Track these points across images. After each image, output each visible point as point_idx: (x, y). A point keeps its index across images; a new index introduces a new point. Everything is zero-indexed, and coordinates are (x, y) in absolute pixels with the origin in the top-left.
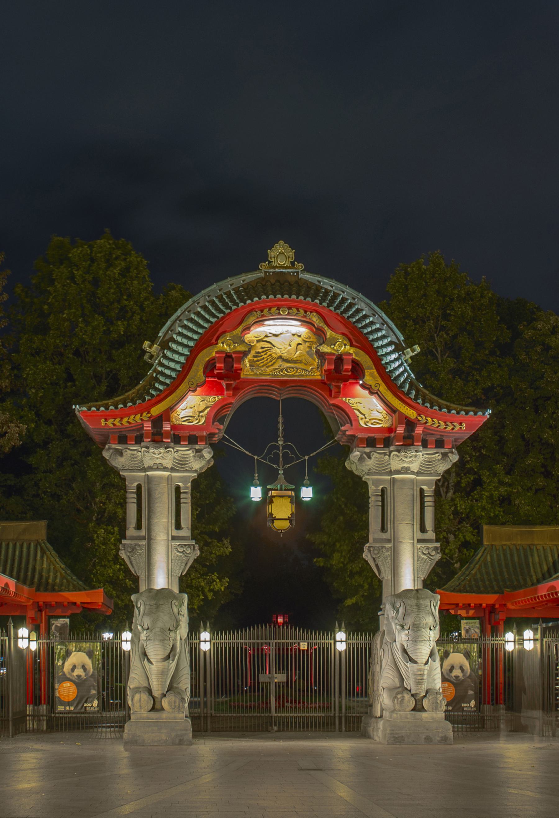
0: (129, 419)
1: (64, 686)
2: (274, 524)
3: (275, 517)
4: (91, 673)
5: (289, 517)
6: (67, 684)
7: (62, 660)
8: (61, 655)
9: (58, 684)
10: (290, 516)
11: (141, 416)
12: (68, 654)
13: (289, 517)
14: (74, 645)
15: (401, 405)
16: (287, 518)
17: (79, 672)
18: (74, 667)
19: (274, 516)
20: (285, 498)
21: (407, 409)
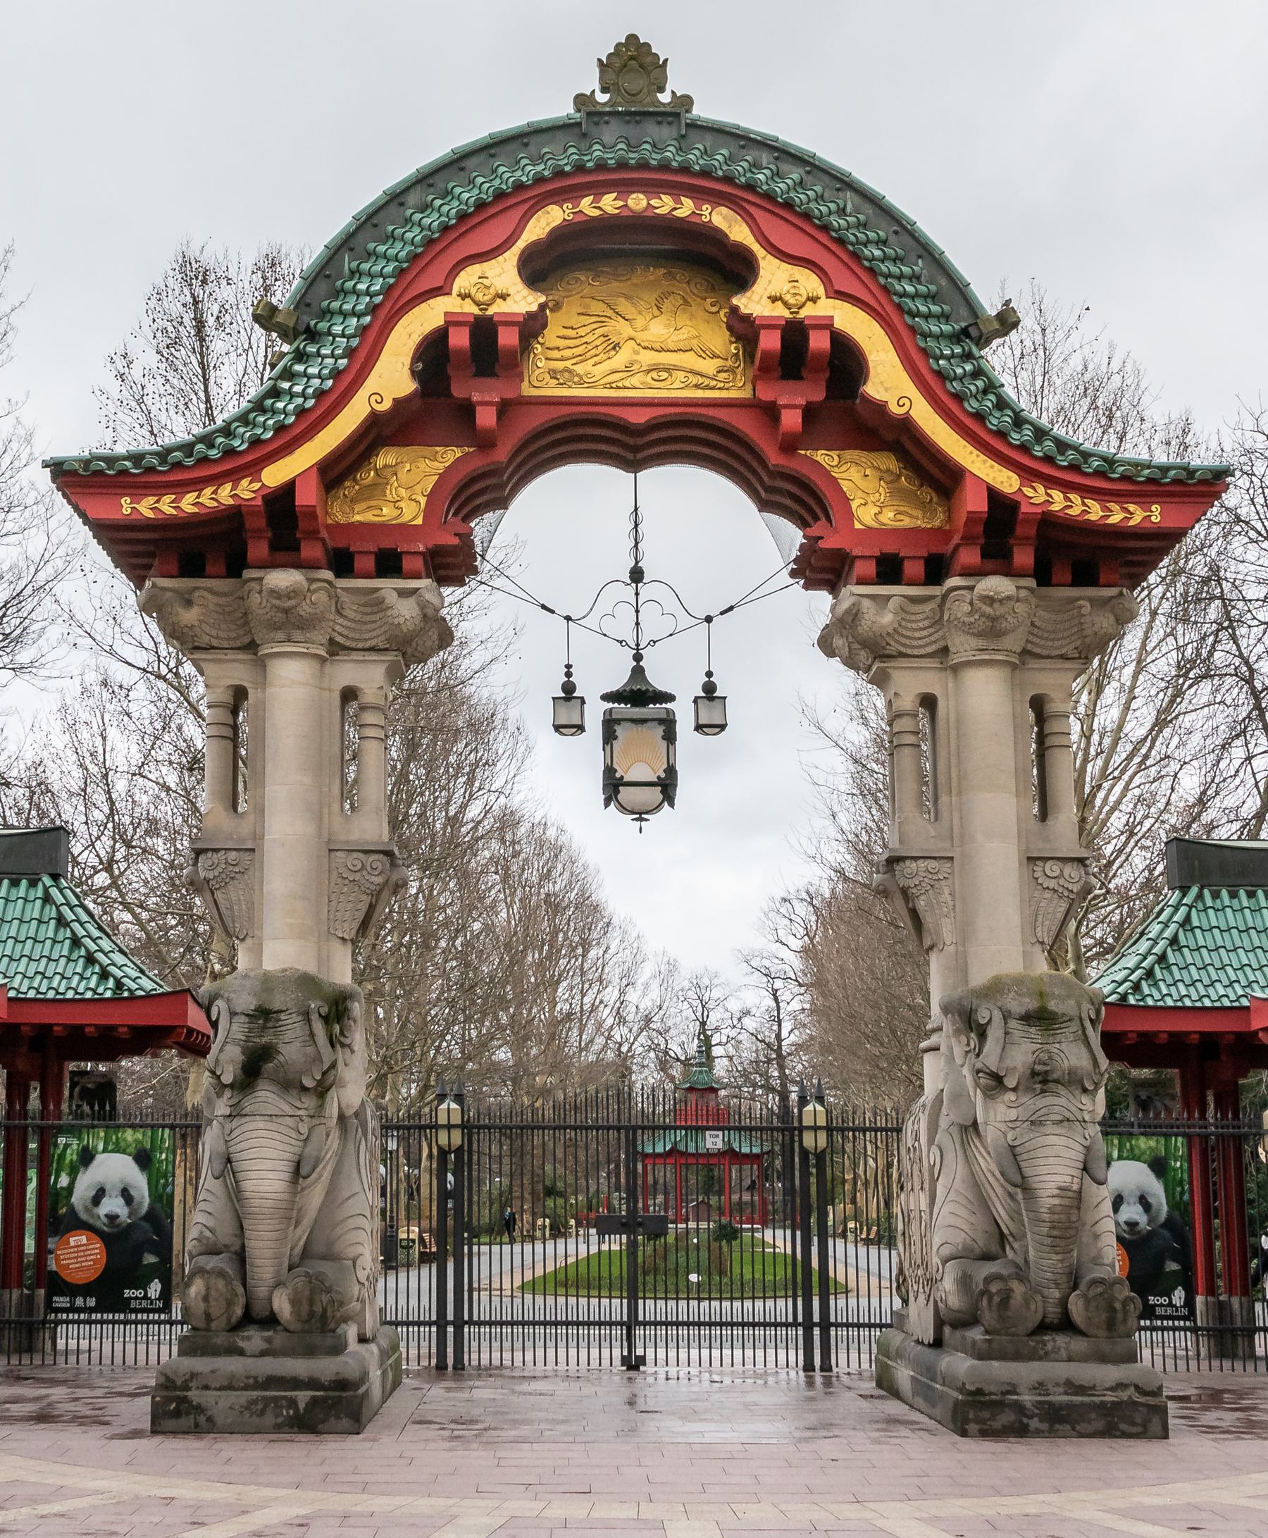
1: (72, 1244)
3: (622, 777)
4: (144, 1208)
5: (659, 777)
6: (78, 1239)
7: (69, 1174)
8: (67, 1161)
9: (57, 1239)
10: (663, 775)
12: (87, 1157)
13: (659, 777)
14: (102, 1134)
15: (974, 456)
17: (113, 1205)
18: (97, 1199)
19: (618, 775)
20: (649, 724)
21: (992, 467)
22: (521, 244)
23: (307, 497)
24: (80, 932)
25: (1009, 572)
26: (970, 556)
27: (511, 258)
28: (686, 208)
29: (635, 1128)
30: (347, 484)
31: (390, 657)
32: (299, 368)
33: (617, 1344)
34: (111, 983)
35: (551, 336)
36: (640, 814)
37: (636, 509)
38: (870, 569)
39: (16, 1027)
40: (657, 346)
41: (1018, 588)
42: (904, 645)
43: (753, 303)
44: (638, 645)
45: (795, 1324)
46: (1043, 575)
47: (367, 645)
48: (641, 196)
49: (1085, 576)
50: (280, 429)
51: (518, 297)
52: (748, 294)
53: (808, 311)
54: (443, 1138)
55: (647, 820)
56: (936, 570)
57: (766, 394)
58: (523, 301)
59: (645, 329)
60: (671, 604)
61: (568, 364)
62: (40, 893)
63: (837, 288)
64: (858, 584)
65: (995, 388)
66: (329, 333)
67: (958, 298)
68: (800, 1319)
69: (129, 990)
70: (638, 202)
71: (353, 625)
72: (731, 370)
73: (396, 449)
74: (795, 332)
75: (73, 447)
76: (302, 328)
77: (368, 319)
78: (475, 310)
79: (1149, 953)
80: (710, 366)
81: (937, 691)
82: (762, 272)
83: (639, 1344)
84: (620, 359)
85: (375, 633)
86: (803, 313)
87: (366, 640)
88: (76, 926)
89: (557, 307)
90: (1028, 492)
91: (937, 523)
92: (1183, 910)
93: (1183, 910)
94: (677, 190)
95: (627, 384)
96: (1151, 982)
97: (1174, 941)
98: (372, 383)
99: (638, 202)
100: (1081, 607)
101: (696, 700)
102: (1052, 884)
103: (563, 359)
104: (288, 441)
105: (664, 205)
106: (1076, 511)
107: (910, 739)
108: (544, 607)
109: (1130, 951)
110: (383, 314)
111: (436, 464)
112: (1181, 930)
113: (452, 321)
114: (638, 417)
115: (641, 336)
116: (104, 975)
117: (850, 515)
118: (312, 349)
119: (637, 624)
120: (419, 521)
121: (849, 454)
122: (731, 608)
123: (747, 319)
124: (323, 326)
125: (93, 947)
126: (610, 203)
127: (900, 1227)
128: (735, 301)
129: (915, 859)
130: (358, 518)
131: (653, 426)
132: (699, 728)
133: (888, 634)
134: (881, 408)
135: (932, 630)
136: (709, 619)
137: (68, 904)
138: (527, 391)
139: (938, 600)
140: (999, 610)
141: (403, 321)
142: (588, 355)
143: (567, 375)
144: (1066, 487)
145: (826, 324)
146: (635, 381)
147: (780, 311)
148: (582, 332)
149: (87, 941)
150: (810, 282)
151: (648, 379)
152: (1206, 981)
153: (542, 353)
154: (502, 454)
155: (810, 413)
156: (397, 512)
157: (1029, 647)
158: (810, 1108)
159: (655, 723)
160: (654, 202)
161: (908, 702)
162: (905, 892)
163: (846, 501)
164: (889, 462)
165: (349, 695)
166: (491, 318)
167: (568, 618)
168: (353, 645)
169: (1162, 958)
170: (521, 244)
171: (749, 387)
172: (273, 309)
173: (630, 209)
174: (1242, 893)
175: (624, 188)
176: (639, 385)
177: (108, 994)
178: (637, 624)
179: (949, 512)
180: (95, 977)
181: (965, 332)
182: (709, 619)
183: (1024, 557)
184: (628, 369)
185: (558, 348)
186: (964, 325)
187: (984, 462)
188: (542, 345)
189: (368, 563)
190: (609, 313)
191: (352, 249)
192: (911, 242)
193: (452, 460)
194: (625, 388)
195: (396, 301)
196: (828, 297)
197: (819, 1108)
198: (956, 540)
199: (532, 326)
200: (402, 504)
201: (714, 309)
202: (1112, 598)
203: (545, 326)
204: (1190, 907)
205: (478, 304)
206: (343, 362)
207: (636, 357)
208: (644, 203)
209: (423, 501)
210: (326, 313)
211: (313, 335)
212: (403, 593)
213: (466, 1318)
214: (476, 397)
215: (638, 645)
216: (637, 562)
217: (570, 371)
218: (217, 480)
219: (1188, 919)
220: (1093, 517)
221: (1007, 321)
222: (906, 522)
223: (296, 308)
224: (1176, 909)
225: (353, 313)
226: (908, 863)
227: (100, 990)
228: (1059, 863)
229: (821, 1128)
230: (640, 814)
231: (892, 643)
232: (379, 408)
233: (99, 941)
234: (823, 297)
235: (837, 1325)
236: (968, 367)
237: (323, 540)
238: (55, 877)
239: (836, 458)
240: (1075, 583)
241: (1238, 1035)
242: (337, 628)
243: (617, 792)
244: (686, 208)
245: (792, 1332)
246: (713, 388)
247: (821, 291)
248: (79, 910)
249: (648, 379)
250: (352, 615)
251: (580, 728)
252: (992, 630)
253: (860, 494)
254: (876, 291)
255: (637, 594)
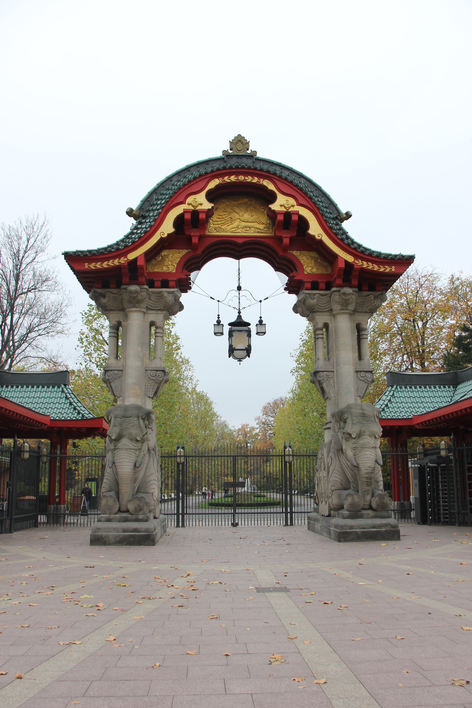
0: (108, 263)
2: (234, 354)
3: (235, 348)
5: (246, 348)
10: (247, 347)
11: (119, 260)
13: (246, 348)
16: (244, 348)
20: (243, 332)
21: (346, 255)
22: (207, 189)
23: (141, 262)
24: (72, 401)
25: (351, 286)
26: (339, 281)
27: (203, 193)
28: (255, 180)
29: (235, 456)
30: (153, 260)
31: (165, 312)
32: (139, 226)
33: (230, 520)
34: (81, 415)
35: (215, 218)
36: (240, 360)
37: (239, 269)
38: (309, 285)
39: (53, 428)
40: (246, 221)
41: (353, 291)
42: (319, 308)
43: (275, 207)
44: (239, 309)
45: (283, 512)
46: (360, 288)
47: (158, 308)
48: (242, 176)
49: (372, 288)
50: (133, 242)
51: (206, 205)
52: (274, 204)
53: (291, 209)
54: (178, 460)
55: (242, 361)
56: (328, 287)
57: (279, 234)
58: (207, 206)
59: (243, 216)
60: (250, 297)
61: (220, 226)
62: (61, 390)
63: (300, 203)
64: (306, 290)
65: (346, 233)
66: (149, 216)
67: (334, 209)
68: (284, 511)
69: (86, 417)
70: (241, 178)
71: (154, 303)
72: (268, 228)
73: (168, 250)
74: (288, 215)
75: (72, 248)
76: (141, 215)
77: (161, 210)
78: (193, 208)
79: (383, 404)
80: (261, 227)
81: (328, 322)
82: (278, 198)
83: (237, 520)
84: (235, 225)
85: (160, 305)
86: (290, 210)
87: (157, 307)
88: (71, 399)
89: (217, 209)
90: (356, 262)
91: (329, 272)
92: (392, 392)
93: (392, 392)
94: (253, 175)
95: (237, 232)
96: (384, 412)
97: (390, 401)
98: (161, 229)
99: (241, 178)
100: (371, 297)
101: (257, 325)
102: (363, 379)
103: (218, 224)
104: (136, 246)
105: (249, 179)
106: (370, 268)
107: (321, 336)
108: (211, 298)
109: (377, 404)
110: (165, 209)
111: (180, 255)
112: (392, 398)
113: (185, 211)
114: (240, 241)
115: (242, 218)
116: (79, 413)
117: (303, 270)
118: (143, 221)
119: (239, 303)
120: (174, 271)
121: (303, 252)
122: (267, 298)
123: (274, 211)
124: (147, 214)
125: (76, 405)
126: (233, 178)
127: (317, 483)
128: (270, 206)
129: (323, 371)
130: (156, 270)
131: (245, 244)
132: (258, 333)
133: (314, 305)
134: (313, 237)
135: (327, 304)
136: (261, 301)
137: (68, 393)
138: (207, 233)
139: (329, 295)
140: (348, 297)
141: (172, 211)
142: (226, 223)
143: (219, 229)
144: (367, 261)
145: (297, 213)
146: (239, 231)
147: (283, 209)
148: (224, 217)
149: (74, 403)
150: (292, 201)
151: (243, 230)
152: (399, 412)
153: (212, 223)
154: (200, 251)
155: (291, 239)
156: (168, 269)
157: (356, 309)
158: (287, 449)
159: (245, 332)
160: (246, 178)
161: (320, 325)
162: (319, 381)
163: (302, 266)
164: (314, 254)
165: (152, 324)
166: (197, 211)
167: (218, 301)
168: (154, 308)
169: (387, 405)
170: (207, 189)
171: (273, 233)
172: (132, 210)
173: (239, 180)
174: (408, 387)
175: (237, 174)
176: (240, 232)
177: (80, 418)
178: (239, 303)
179: (332, 269)
180: (76, 414)
181: (336, 218)
182: (261, 301)
183: (355, 282)
184: (237, 227)
185: (217, 221)
186: (336, 216)
187: (344, 253)
188: (212, 220)
189: (159, 284)
190: (232, 211)
191: (156, 193)
192: (320, 192)
193: (185, 253)
194: (236, 232)
195: (169, 205)
196: (297, 205)
197: (290, 449)
198: (335, 276)
199: (209, 213)
200: (169, 266)
201: (263, 210)
202: (380, 295)
203: (213, 214)
204: (394, 391)
205: (193, 206)
206: (153, 223)
207: (240, 224)
208: (243, 178)
209: (176, 265)
210: (149, 211)
211: (144, 217)
212: (169, 293)
213: (185, 512)
214: (192, 234)
215: (239, 309)
216: (239, 284)
217: (220, 228)
218: (114, 258)
219: (393, 394)
220: (375, 269)
221: (348, 216)
222: (319, 272)
223: (139, 210)
224: (390, 392)
225: (156, 210)
226: (320, 373)
227: (77, 417)
228: (365, 373)
229: (291, 455)
230: (240, 360)
231: (316, 308)
232: (163, 236)
233: (77, 403)
234: (296, 205)
235: (295, 512)
236: (338, 227)
237: (145, 276)
238: (65, 385)
239: (299, 253)
240: (369, 290)
241: (409, 427)
242: (149, 303)
243: (233, 352)
244: (255, 180)
245: (281, 514)
246: (263, 233)
247: (295, 204)
248: (72, 395)
249: (243, 230)
250: (154, 300)
251: (222, 334)
252: (345, 304)
253: (306, 264)
254: (311, 204)
255: (239, 294)
